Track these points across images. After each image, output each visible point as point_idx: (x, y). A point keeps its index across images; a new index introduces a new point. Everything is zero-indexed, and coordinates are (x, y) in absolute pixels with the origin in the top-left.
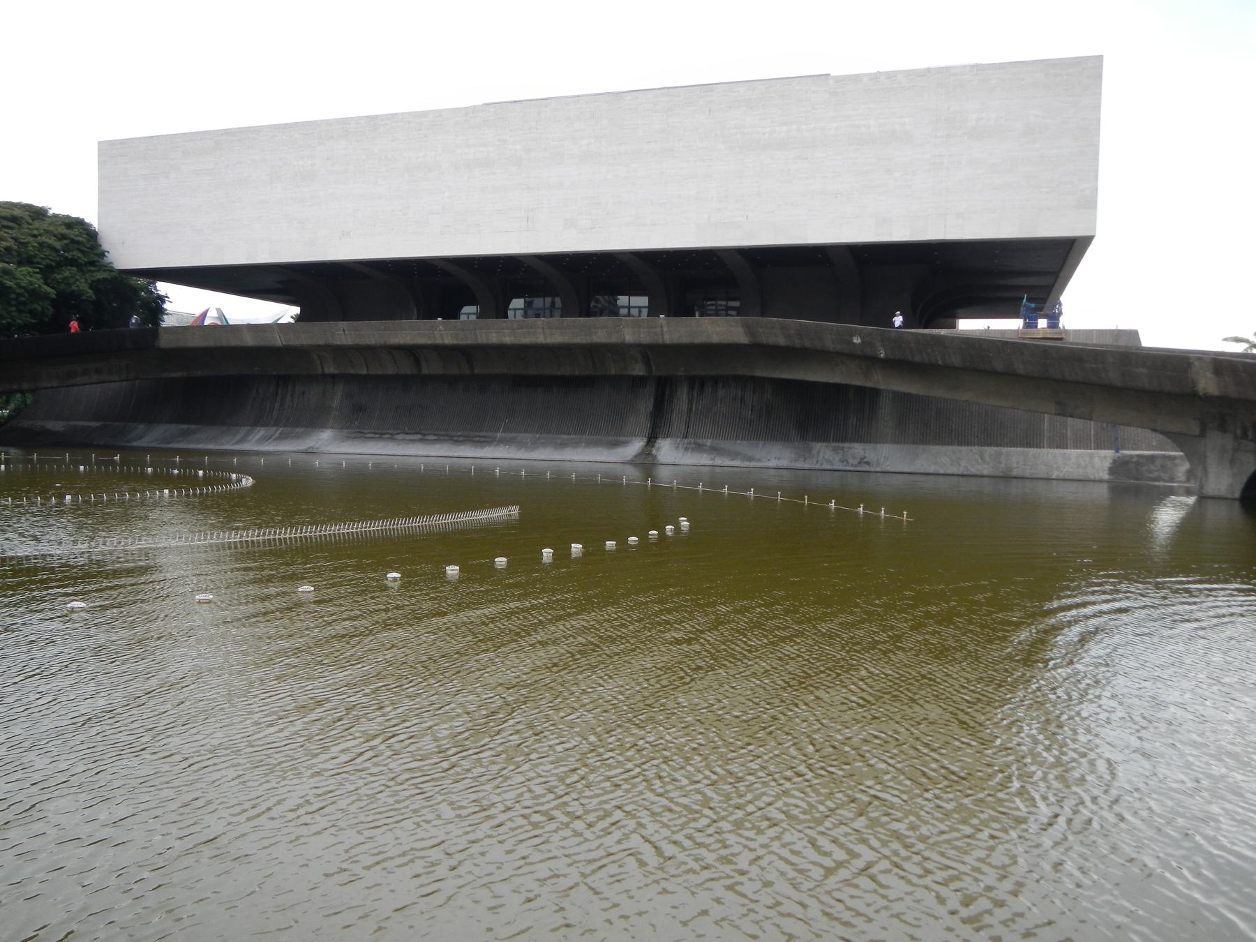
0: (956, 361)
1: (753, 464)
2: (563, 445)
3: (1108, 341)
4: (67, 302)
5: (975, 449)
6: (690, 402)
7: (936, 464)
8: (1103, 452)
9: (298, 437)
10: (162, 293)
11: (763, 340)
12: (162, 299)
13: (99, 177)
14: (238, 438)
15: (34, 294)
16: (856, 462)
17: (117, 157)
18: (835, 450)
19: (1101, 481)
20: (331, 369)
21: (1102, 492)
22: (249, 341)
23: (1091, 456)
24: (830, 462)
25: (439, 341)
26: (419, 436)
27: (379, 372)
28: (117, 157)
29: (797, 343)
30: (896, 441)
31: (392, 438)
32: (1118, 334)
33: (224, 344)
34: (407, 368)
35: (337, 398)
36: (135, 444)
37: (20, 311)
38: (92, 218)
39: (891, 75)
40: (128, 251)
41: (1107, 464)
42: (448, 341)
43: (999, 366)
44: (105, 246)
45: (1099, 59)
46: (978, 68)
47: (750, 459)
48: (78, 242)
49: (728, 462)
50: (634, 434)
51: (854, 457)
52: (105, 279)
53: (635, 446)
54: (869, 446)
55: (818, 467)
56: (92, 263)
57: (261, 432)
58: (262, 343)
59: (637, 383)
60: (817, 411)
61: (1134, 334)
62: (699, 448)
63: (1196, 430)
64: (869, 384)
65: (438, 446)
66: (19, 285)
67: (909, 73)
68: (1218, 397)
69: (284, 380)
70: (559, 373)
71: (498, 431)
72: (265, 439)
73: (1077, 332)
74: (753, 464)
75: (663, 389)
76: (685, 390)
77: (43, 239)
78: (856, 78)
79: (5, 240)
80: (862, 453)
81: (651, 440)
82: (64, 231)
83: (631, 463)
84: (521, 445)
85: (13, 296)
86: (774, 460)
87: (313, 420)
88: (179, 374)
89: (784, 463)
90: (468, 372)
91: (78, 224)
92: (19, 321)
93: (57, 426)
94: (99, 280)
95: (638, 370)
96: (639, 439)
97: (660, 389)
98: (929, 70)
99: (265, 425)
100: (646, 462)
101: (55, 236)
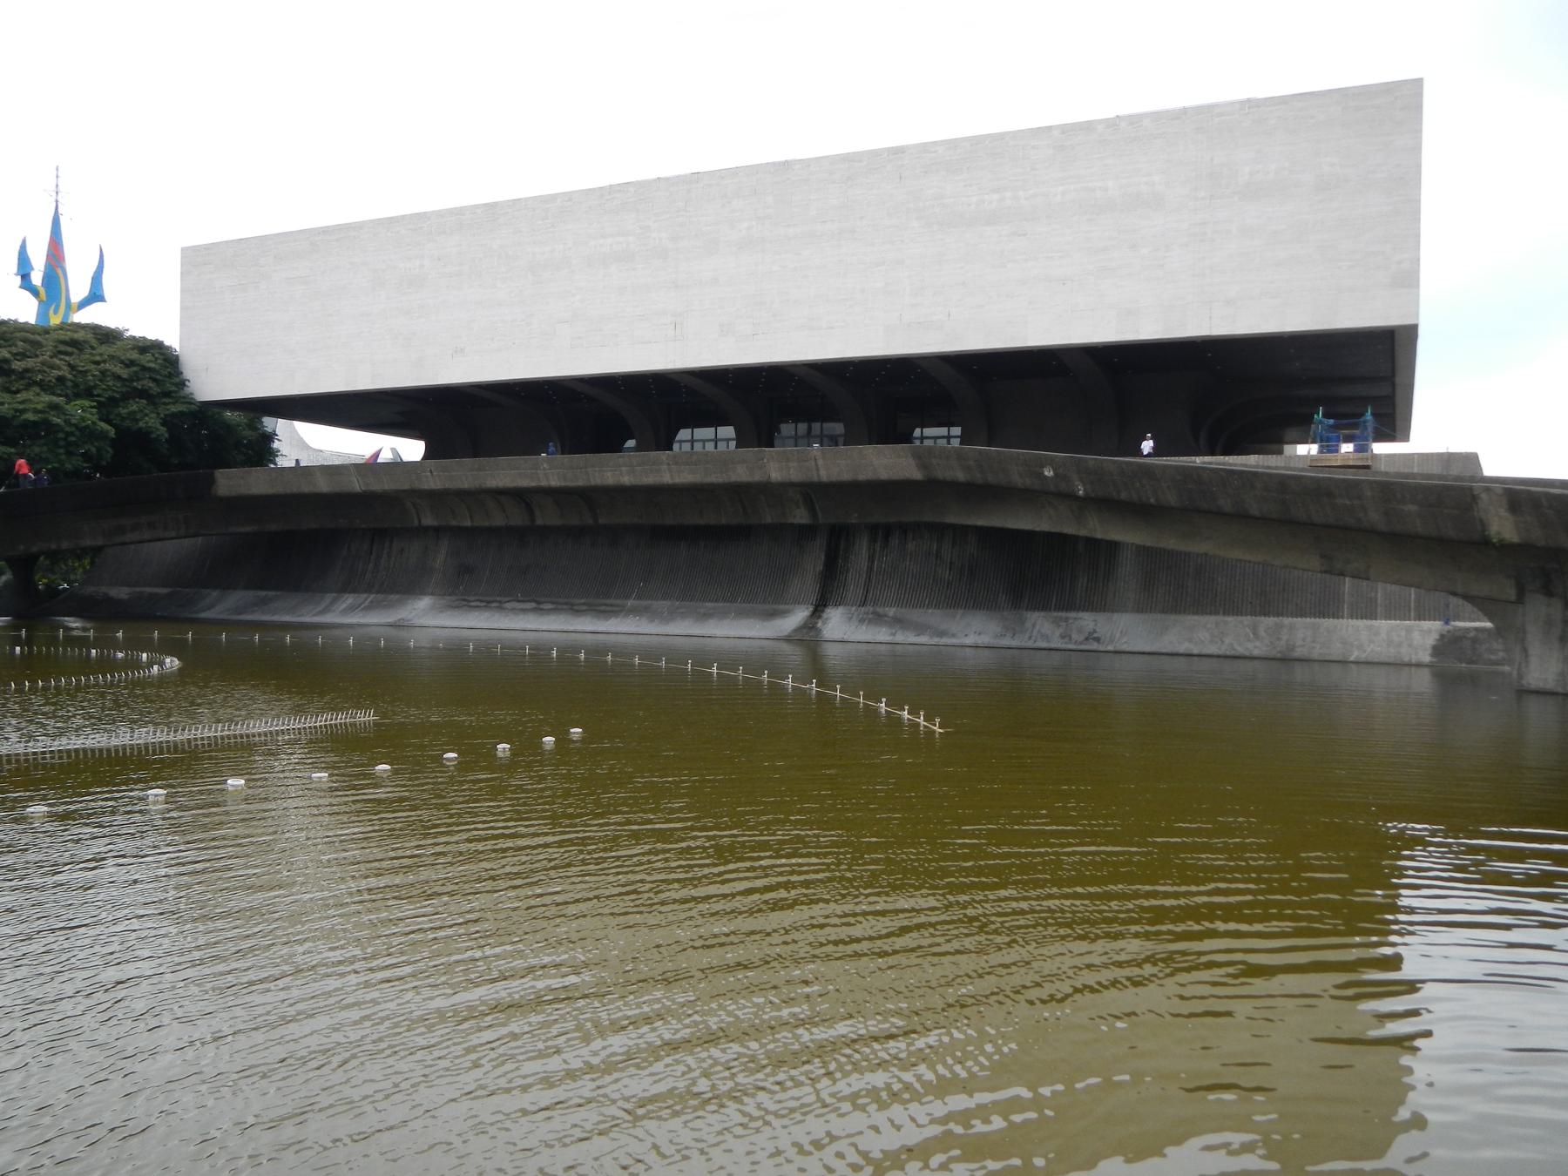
0: (1171, 499)
1: (944, 641)
2: (706, 616)
3: (1436, 469)
4: (132, 442)
5: (1248, 620)
6: (871, 559)
7: (1190, 640)
8: (1426, 624)
9: (390, 606)
10: (269, 430)
11: (940, 474)
12: (270, 437)
13: (183, 291)
14: (323, 606)
15: (89, 434)
16: (1082, 638)
17: (204, 266)
18: (1057, 622)
19: (1419, 665)
20: (428, 521)
21: (1423, 682)
22: (323, 486)
23: (1409, 630)
24: (1046, 637)
25: (544, 483)
26: (533, 605)
27: (487, 524)
28: (204, 266)
29: (978, 478)
30: (1139, 609)
31: (500, 608)
32: (1449, 458)
33: (295, 490)
34: (518, 519)
35: (441, 557)
36: (203, 615)
37: (70, 454)
38: (172, 340)
39: (1134, 120)
40: (218, 377)
41: (1431, 641)
43: (1226, 504)
46: (1251, 105)
47: (942, 634)
48: (150, 369)
49: (913, 639)
50: (798, 602)
51: (1080, 631)
52: (182, 413)
53: (798, 616)
54: (1101, 618)
55: (1030, 644)
56: (167, 394)
57: (349, 600)
58: (337, 489)
59: (804, 533)
60: (1034, 570)
61: (1472, 459)
62: (878, 619)
63: (1511, 593)
64: (1083, 533)
65: (552, 617)
66: (67, 422)
67: (1157, 116)
68: (1519, 545)
69: (380, 535)
70: (702, 522)
71: (627, 597)
72: (352, 609)
74: (944, 641)
75: (837, 541)
76: (865, 543)
78: (1088, 127)
79: (59, 369)
80: (1091, 625)
81: (818, 611)
82: (135, 355)
83: (788, 639)
84: (653, 615)
85: (61, 435)
86: (973, 635)
87: (406, 585)
88: (248, 529)
89: (985, 639)
90: (590, 522)
91: (157, 348)
92: (68, 466)
93: (121, 593)
94: (174, 415)
95: (800, 517)
96: (803, 607)
97: (832, 542)
98: (1185, 110)
99: (354, 591)
100: (808, 637)
101: (122, 362)
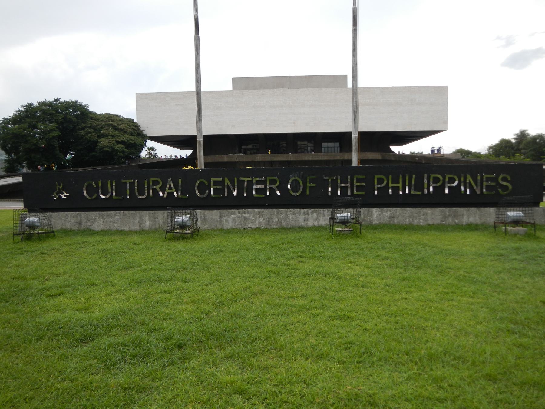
17: (140, 97)
25: (289, 159)
28: (140, 97)
39: (396, 88)
42: (292, 160)
44: (141, 129)
45: (447, 87)
58: (230, 161)
73: (447, 154)
77: (132, 127)
78: (387, 88)
91: (131, 121)
